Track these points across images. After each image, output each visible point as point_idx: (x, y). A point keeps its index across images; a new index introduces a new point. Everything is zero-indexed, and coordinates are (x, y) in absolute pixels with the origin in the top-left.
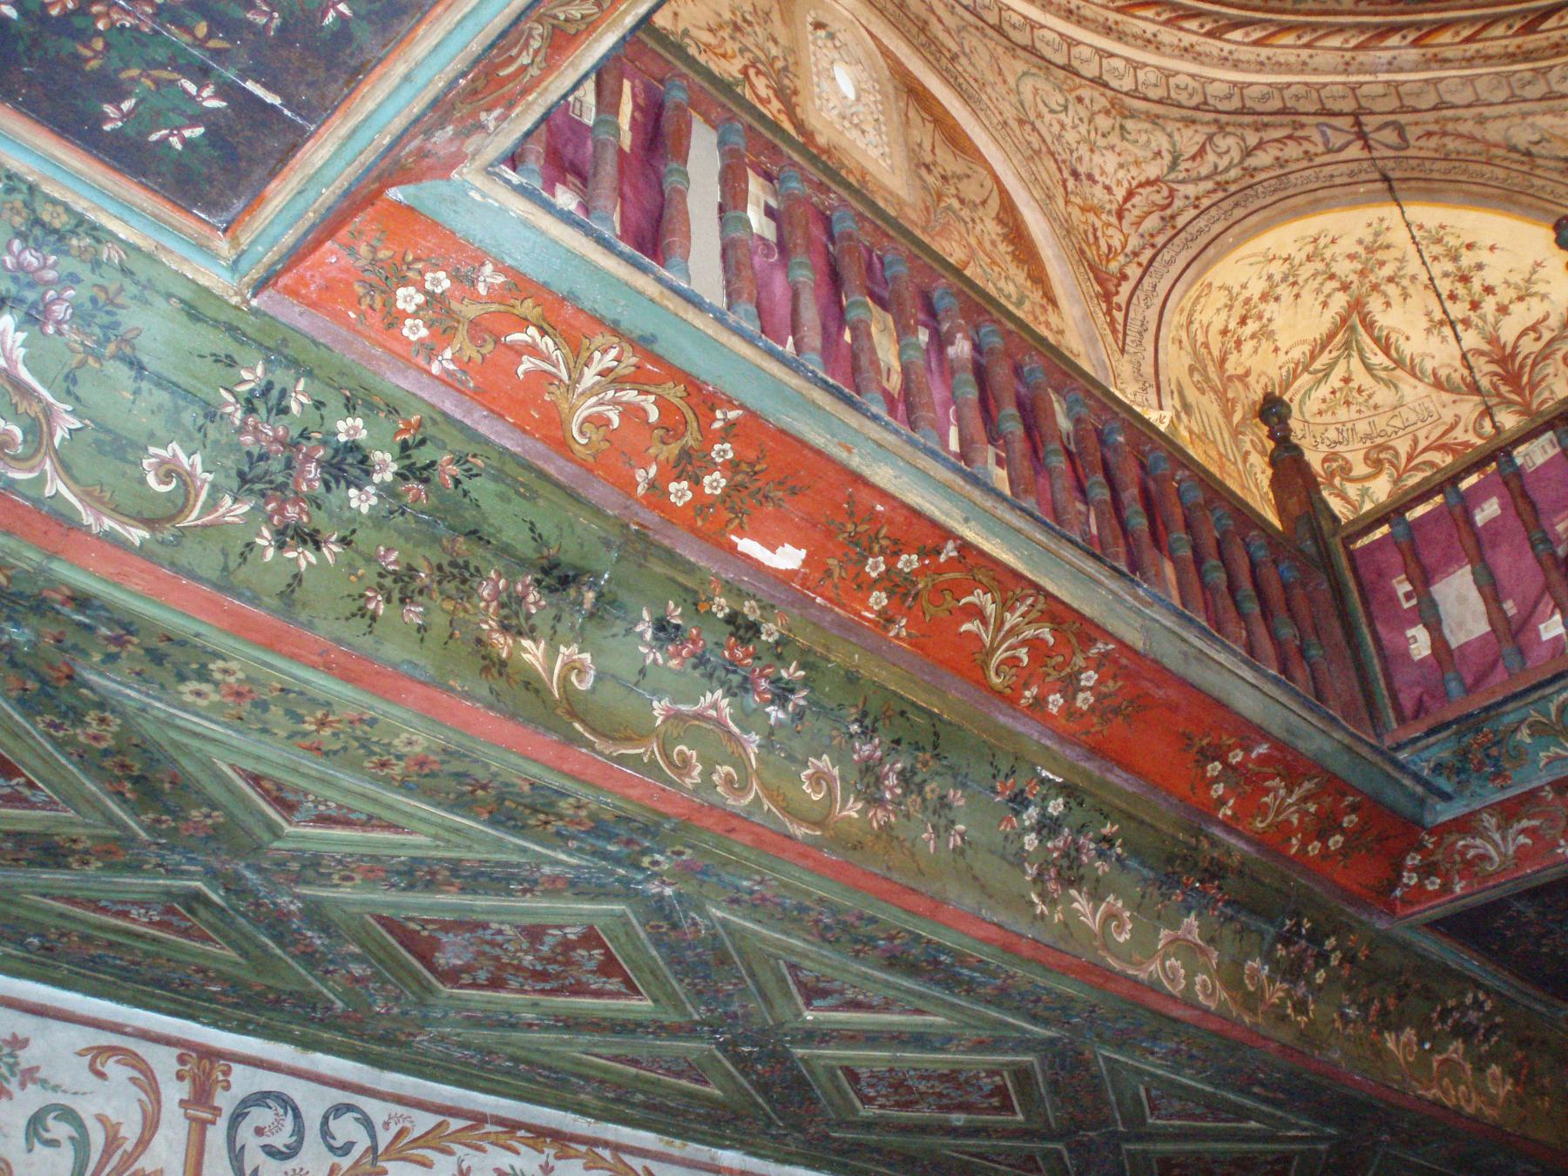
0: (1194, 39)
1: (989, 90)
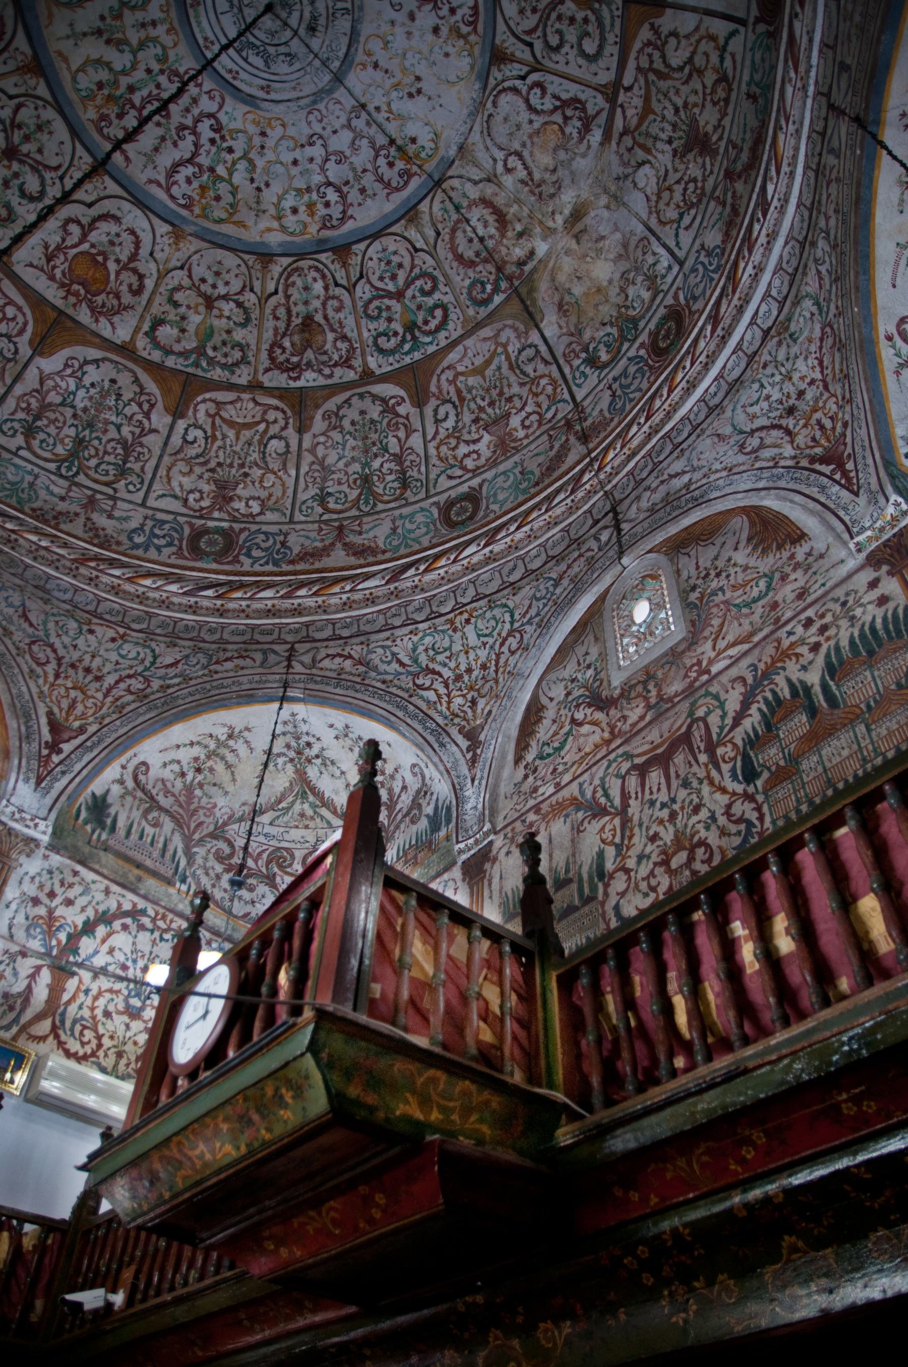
0: (764, 232)
1: (717, 466)
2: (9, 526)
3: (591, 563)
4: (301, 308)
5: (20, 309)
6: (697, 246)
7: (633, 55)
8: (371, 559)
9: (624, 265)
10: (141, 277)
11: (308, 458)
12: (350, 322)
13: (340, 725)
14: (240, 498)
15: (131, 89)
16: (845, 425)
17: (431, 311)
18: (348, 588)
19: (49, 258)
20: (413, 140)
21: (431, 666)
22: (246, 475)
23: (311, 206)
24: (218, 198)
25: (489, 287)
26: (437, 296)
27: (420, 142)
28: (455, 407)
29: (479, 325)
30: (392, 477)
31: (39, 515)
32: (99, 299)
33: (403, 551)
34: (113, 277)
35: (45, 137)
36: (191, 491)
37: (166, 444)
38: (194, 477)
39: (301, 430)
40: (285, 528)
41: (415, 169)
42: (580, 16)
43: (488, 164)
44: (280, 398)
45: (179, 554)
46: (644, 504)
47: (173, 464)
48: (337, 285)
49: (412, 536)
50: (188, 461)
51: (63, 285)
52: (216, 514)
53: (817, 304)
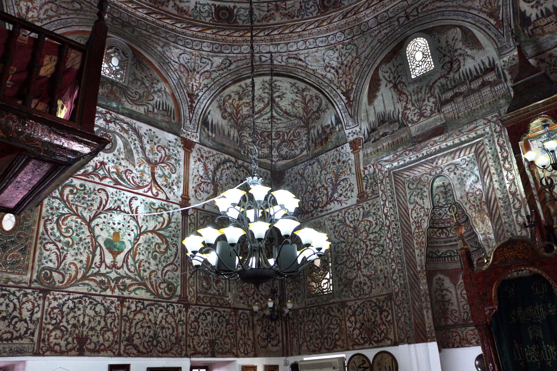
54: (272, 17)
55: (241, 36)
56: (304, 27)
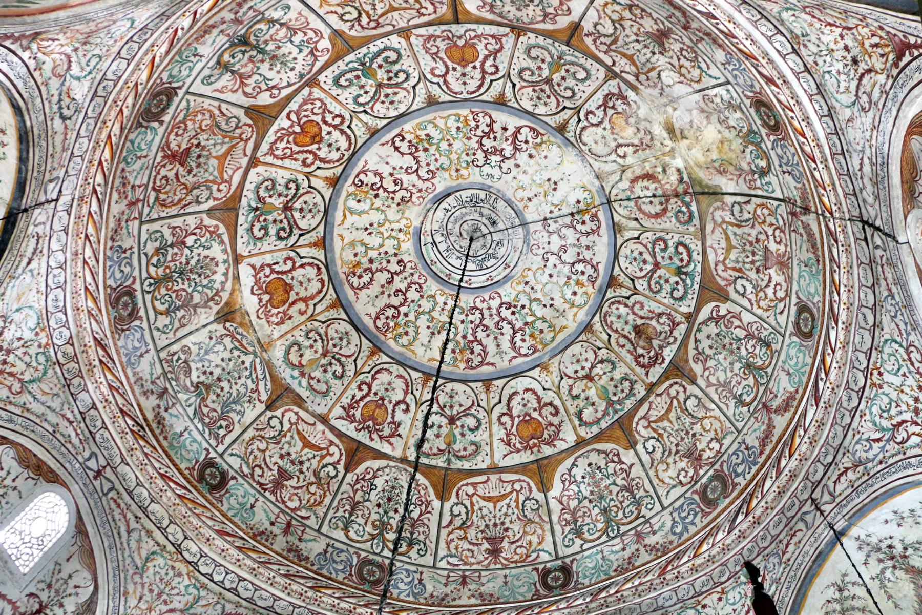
0: (727, 23)
1: (868, 134)
2: (612, 591)
3: (890, 263)
4: (628, 328)
5: (519, 480)
6: (722, 68)
7: (597, 52)
8: (795, 403)
9: (714, 118)
10: (551, 404)
11: (711, 391)
12: (654, 306)
13: (890, 516)
14: (703, 450)
15: (464, 337)
16: (881, 28)
17: (677, 252)
18: (802, 433)
19: (509, 445)
20: (578, 202)
21: (894, 422)
22: (694, 435)
23: (578, 283)
24: (542, 331)
25: (684, 209)
26: (670, 243)
27: (581, 199)
28: (742, 278)
29: (703, 229)
30: (758, 348)
31: (620, 570)
32: (546, 436)
33: (805, 379)
34: (540, 419)
35: (456, 398)
36: (679, 475)
37: (643, 466)
38: (672, 466)
39: (693, 382)
40: (739, 439)
41: (593, 210)
42: (563, 73)
43: (614, 167)
44: (667, 379)
45: (705, 515)
46: (870, 200)
47: (657, 471)
48: (628, 298)
49: (800, 365)
50: (661, 461)
51: (525, 448)
52: (702, 472)
53: (787, 9)
54: (123, 195)
55: (109, 137)
56: (92, 262)
